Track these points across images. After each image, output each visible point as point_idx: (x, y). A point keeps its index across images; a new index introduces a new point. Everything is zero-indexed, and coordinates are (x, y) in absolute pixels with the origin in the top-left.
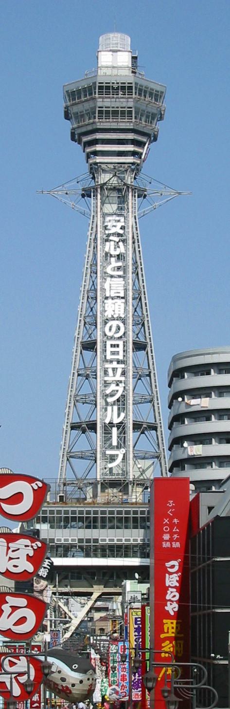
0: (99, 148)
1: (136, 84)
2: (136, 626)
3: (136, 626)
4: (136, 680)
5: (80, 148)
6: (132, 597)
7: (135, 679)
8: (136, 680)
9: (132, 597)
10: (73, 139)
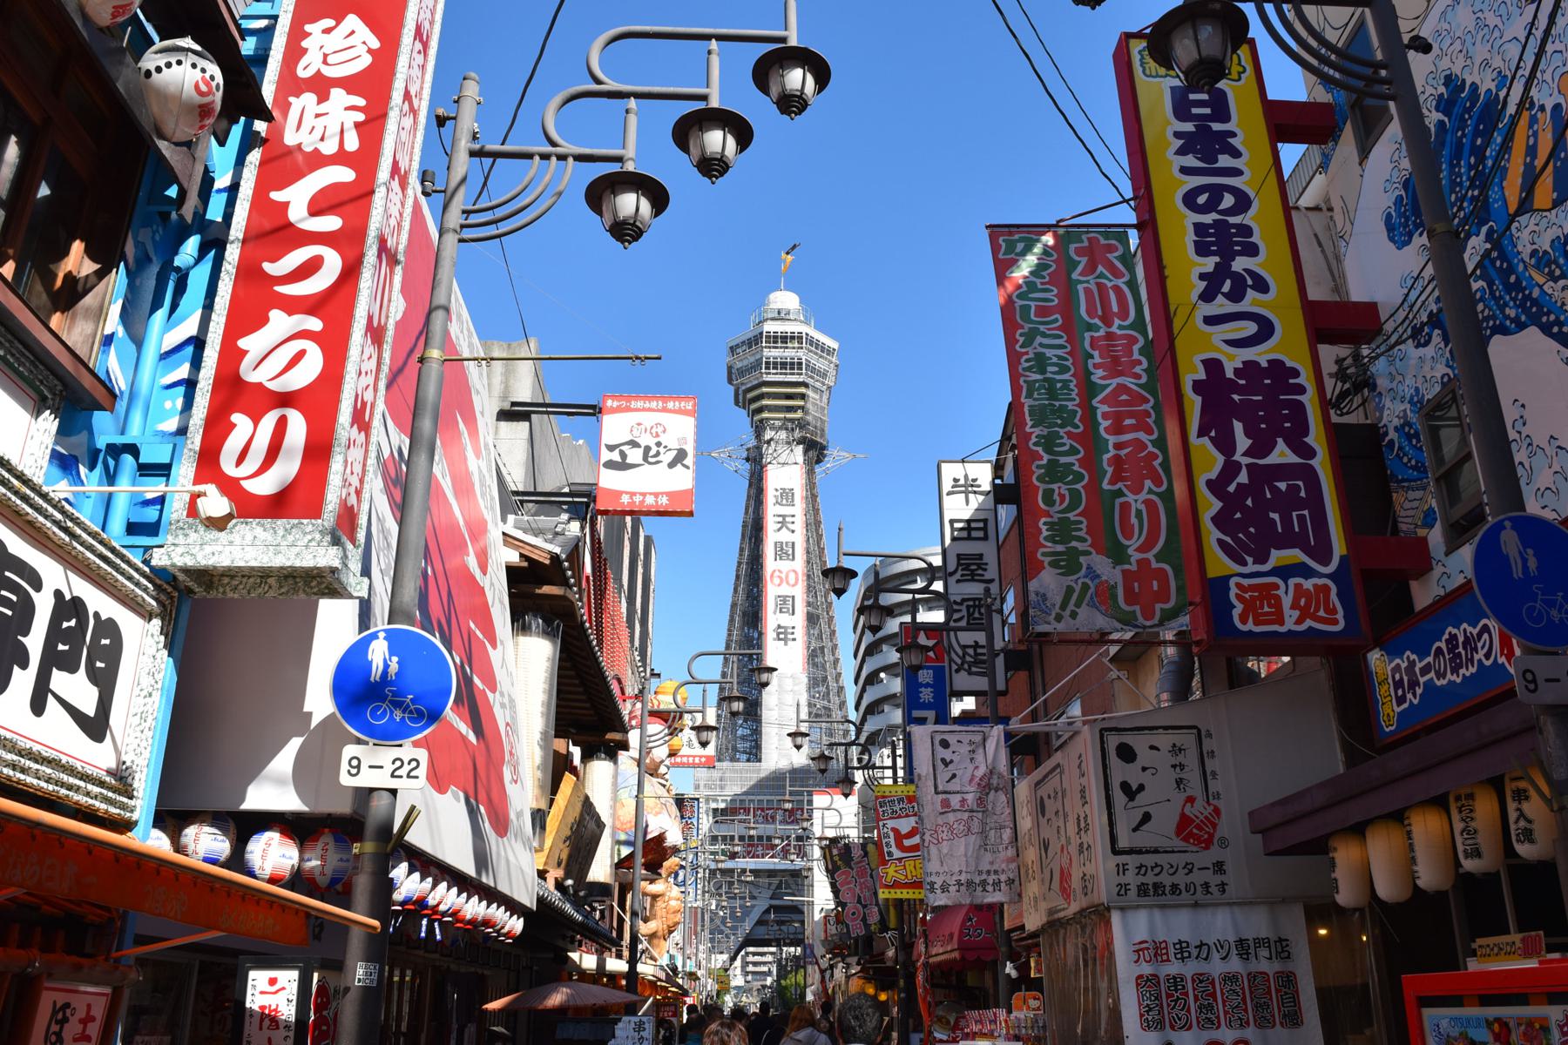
0: (765, 402)
1: (807, 334)
2: (1189, 127)
3: (1189, 127)
4: (1243, 478)
5: (744, 412)
6: (956, 480)
7: (1231, 469)
8: (1243, 478)
9: (956, 480)
10: (737, 403)
